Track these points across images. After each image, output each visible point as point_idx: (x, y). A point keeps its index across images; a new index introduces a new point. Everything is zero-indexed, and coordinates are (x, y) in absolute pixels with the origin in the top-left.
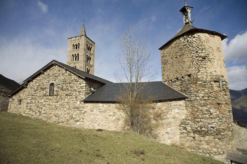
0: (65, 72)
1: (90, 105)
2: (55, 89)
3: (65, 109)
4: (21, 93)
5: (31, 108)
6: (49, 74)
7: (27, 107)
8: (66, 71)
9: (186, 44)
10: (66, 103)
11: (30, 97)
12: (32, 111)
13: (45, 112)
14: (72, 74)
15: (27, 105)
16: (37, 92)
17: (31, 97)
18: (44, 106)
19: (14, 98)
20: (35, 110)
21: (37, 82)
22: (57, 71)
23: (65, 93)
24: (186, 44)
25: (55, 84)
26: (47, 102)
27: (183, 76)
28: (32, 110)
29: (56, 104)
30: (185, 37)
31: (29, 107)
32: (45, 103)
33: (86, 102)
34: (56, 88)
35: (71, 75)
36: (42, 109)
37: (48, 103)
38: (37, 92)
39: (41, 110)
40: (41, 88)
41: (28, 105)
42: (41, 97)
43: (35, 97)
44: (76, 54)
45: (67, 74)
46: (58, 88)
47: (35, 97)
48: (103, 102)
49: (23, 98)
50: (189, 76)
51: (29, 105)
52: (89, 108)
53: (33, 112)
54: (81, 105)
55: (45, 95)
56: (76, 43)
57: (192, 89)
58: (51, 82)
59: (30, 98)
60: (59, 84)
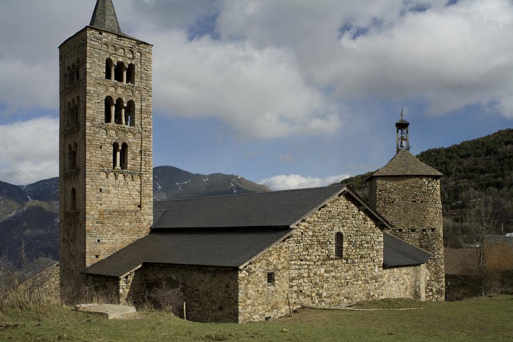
0: (357, 212)
1: (388, 271)
2: (345, 245)
3: (360, 282)
4: (271, 255)
5: (301, 288)
6: (330, 211)
7: (291, 289)
8: (359, 211)
9: (431, 190)
10: (360, 272)
11: (296, 262)
12: (303, 296)
13: (329, 293)
14: (369, 219)
15: (291, 284)
16: (311, 251)
17: (298, 262)
18: (326, 281)
19: (253, 269)
20: (309, 293)
21: (307, 228)
22: (344, 207)
23: (360, 253)
24: (431, 190)
25: (344, 234)
26: (332, 271)
27: (425, 228)
28: (304, 294)
29: (346, 274)
30: (430, 179)
31: (295, 288)
32: (326, 275)
33: (385, 267)
34: (346, 243)
35: (366, 220)
36: (323, 288)
37: (333, 274)
38: (311, 251)
39: (321, 291)
40: (319, 241)
41: (293, 284)
42: (319, 263)
43: (308, 263)
44: (124, 99)
45: (361, 217)
46: (350, 242)
47: (308, 263)
48: (397, 267)
49: (280, 267)
50: (433, 230)
51: (295, 283)
52: (386, 276)
53: (305, 297)
54: (380, 273)
55: (328, 258)
56: (121, 60)
57: (435, 245)
58: (336, 230)
59: (297, 267)
60: (351, 236)
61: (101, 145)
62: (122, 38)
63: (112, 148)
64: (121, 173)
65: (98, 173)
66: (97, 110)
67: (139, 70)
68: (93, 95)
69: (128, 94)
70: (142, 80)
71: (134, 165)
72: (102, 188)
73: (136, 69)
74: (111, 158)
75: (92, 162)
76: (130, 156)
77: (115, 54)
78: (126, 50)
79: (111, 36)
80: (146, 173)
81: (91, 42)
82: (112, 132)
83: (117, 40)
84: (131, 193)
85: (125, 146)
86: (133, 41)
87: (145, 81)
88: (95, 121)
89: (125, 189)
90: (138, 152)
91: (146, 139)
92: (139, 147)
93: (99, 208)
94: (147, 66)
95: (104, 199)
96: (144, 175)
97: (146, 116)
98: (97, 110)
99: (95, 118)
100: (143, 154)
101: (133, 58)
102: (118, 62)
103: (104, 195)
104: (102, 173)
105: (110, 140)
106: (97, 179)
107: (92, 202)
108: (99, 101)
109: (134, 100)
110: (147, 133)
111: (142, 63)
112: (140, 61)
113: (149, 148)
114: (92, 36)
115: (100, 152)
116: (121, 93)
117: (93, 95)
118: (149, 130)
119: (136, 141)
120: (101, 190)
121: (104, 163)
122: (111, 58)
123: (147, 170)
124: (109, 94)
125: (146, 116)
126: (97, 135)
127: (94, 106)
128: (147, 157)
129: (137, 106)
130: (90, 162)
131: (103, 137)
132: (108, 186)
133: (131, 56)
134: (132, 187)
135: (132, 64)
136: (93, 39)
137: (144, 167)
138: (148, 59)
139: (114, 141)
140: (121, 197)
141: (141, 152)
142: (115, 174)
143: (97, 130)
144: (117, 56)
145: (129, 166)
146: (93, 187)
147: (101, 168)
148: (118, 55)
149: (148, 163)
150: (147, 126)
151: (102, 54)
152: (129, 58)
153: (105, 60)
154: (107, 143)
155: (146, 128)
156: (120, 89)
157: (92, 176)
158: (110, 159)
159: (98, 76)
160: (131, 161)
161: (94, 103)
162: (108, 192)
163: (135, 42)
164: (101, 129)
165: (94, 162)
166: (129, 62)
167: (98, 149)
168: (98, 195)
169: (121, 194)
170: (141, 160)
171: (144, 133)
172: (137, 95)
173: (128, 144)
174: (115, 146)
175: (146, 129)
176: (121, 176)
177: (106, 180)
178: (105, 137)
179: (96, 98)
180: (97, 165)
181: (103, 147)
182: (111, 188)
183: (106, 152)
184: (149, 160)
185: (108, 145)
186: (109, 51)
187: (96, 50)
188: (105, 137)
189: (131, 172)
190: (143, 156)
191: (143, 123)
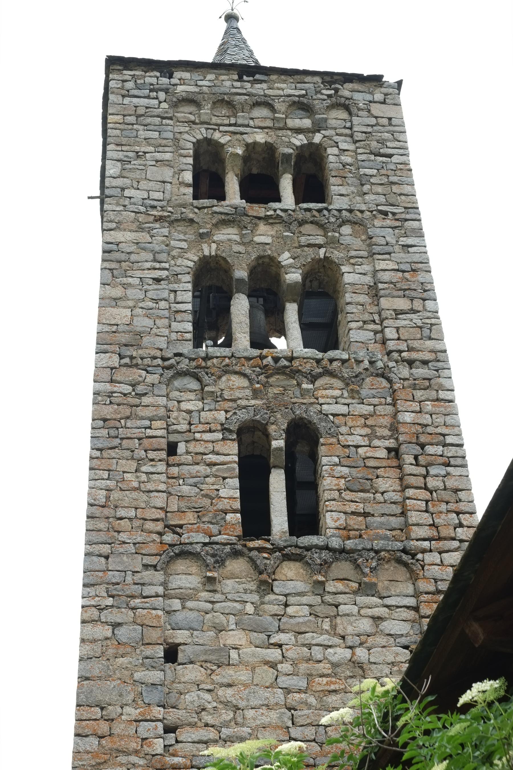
44: (285, 259)
56: (260, 137)
61: (173, 438)
62: (257, 77)
63: (233, 448)
64: (287, 558)
65: (153, 560)
66: (151, 304)
67: (347, 159)
68: (133, 257)
69: (303, 240)
70: (366, 188)
71: (366, 515)
72: (180, 636)
73: (331, 158)
74: (231, 491)
75: (121, 513)
76: (332, 475)
77: (235, 125)
78: (277, 106)
79: (211, 77)
80: (441, 544)
81: (127, 100)
82: (235, 385)
83: (238, 84)
84: (361, 653)
85: (304, 436)
86: (308, 79)
87: (380, 189)
88: (139, 347)
89: (323, 639)
90: (383, 454)
91: (418, 394)
92: (386, 432)
93: (158, 746)
94: (382, 142)
95: (191, 698)
96: (429, 558)
97: (403, 304)
98: (151, 304)
99: (139, 334)
100: (409, 459)
101: (317, 128)
102: (251, 148)
103: (191, 673)
104: (181, 565)
105: (221, 416)
106: (148, 590)
107: (113, 711)
108: (157, 274)
109: (336, 255)
110: (420, 372)
111: (358, 136)
112: (348, 132)
113: (444, 431)
114: (130, 85)
115: (161, 467)
116: (269, 240)
117: (133, 257)
118: (427, 356)
119: (366, 409)
120: (171, 654)
121: (190, 517)
122: (217, 136)
123: (445, 532)
124: (209, 250)
125: (403, 304)
126: (146, 400)
127: (135, 293)
128: (433, 471)
129: (350, 276)
130: (106, 512)
131: (185, 406)
132: (220, 629)
133: (307, 123)
134: (365, 625)
135: (311, 144)
136: (132, 92)
137: (426, 518)
138: (385, 121)
139: (243, 416)
140: (303, 684)
141: (395, 452)
142: (252, 560)
143: (151, 379)
144: (241, 129)
145: (331, 520)
146: (122, 633)
147: (169, 538)
148: (248, 126)
149: (446, 495)
150: (416, 344)
151: (176, 130)
152: (298, 131)
153: (190, 145)
154: (201, 428)
155: (410, 349)
156: (262, 227)
157: (116, 577)
158: (223, 493)
159: (158, 195)
160: (348, 495)
161: (137, 281)
162: (219, 659)
163: (318, 79)
164: (170, 373)
165: (132, 513)
166: (300, 140)
167: (151, 455)
168: (156, 676)
169: (294, 664)
170: (404, 488)
171: (405, 371)
172: (346, 240)
173: (322, 426)
174: (251, 438)
175: (414, 355)
176: (291, 577)
177: (204, 595)
178: (194, 405)
179: (148, 265)
180: (149, 526)
181: (181, 448)
182: (235, 637)
183: (202, 469)
184: (451, 483)
185: (207, 436)
186: (204, 118)
187: (149, 120)
188: (194, 405)
189: (350, 544)
190: (409, 469)
191: (390, 333)
